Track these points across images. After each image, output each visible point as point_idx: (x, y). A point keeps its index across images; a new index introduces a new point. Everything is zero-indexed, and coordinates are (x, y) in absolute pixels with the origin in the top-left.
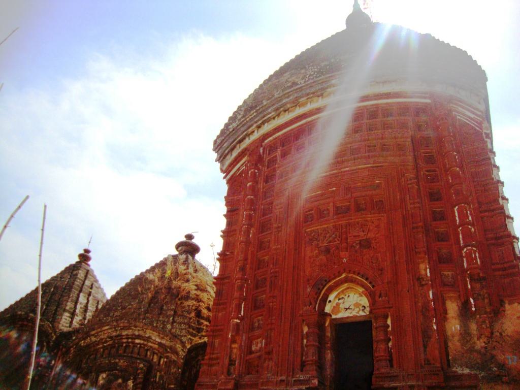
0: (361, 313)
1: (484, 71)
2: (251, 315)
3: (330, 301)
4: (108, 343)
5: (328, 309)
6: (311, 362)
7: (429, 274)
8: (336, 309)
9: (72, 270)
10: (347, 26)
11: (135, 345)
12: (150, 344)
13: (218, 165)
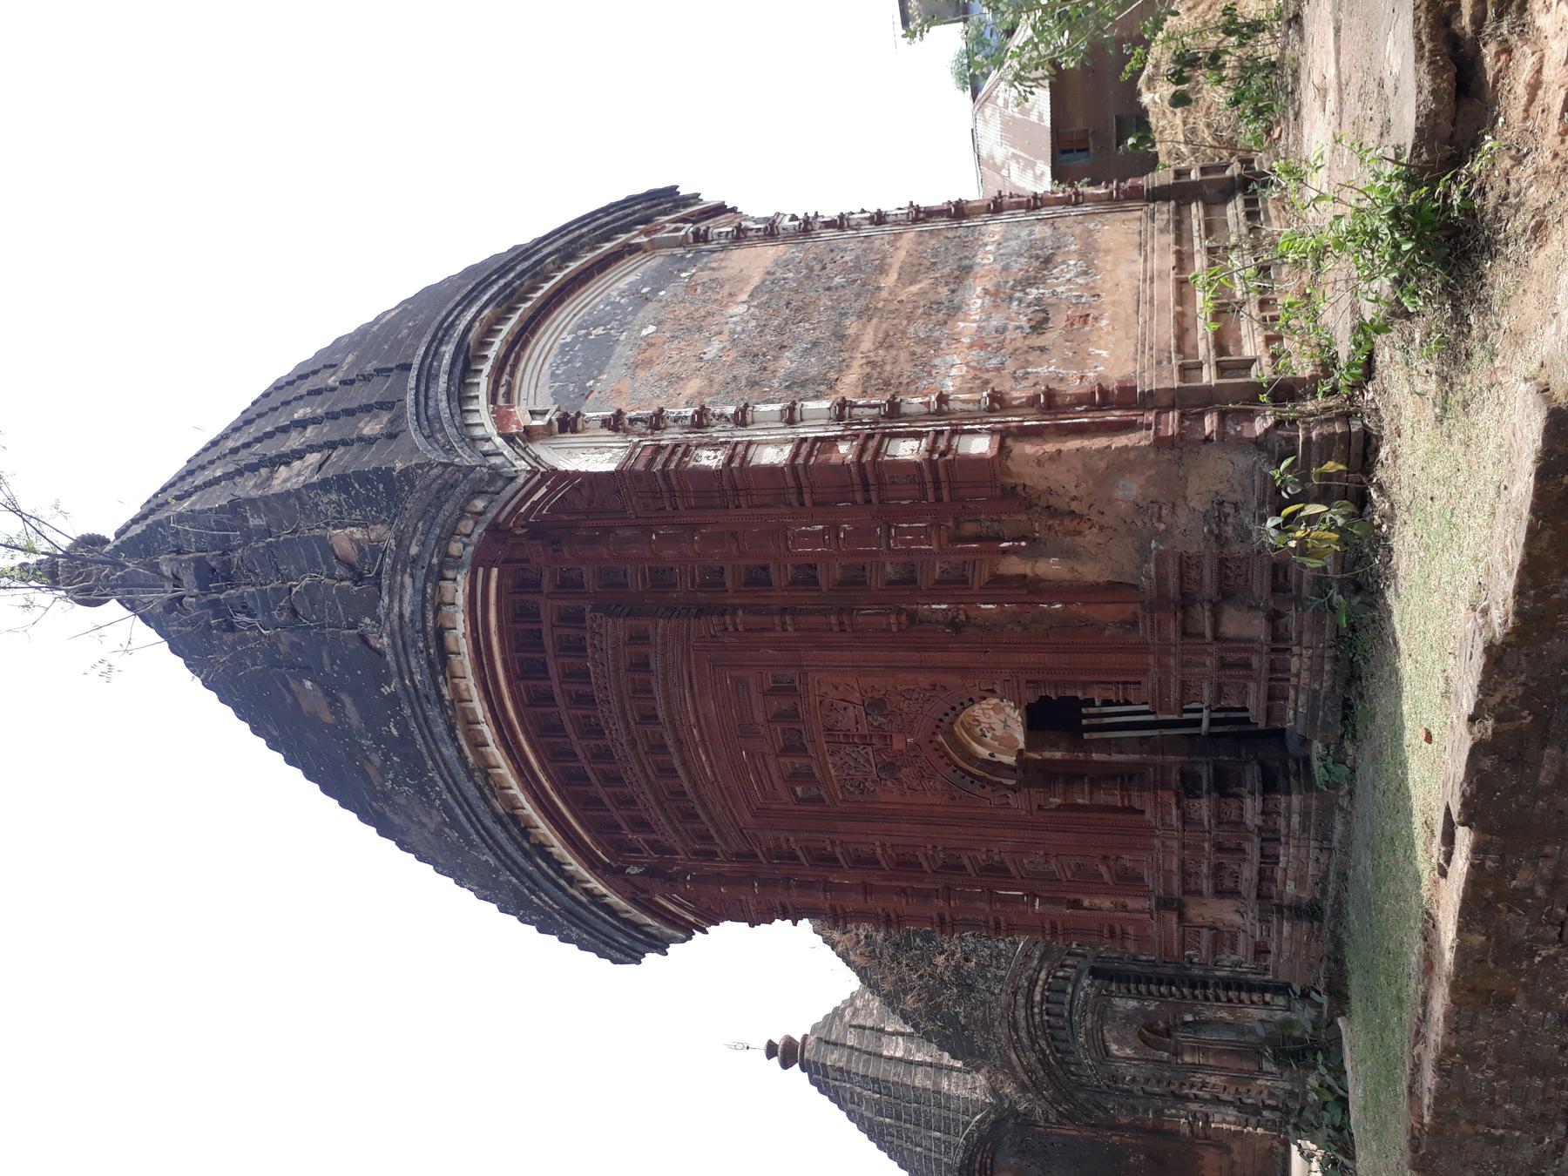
2: (1023, 878)
3: (992, 755)
4: (1044, 1046)
5: (1009, 760)
6: (1126, 800)
7: (944, 607)
8: (1007, 742)
9: (825, 1080)
12: (1043, 975)
13: (673, 948)
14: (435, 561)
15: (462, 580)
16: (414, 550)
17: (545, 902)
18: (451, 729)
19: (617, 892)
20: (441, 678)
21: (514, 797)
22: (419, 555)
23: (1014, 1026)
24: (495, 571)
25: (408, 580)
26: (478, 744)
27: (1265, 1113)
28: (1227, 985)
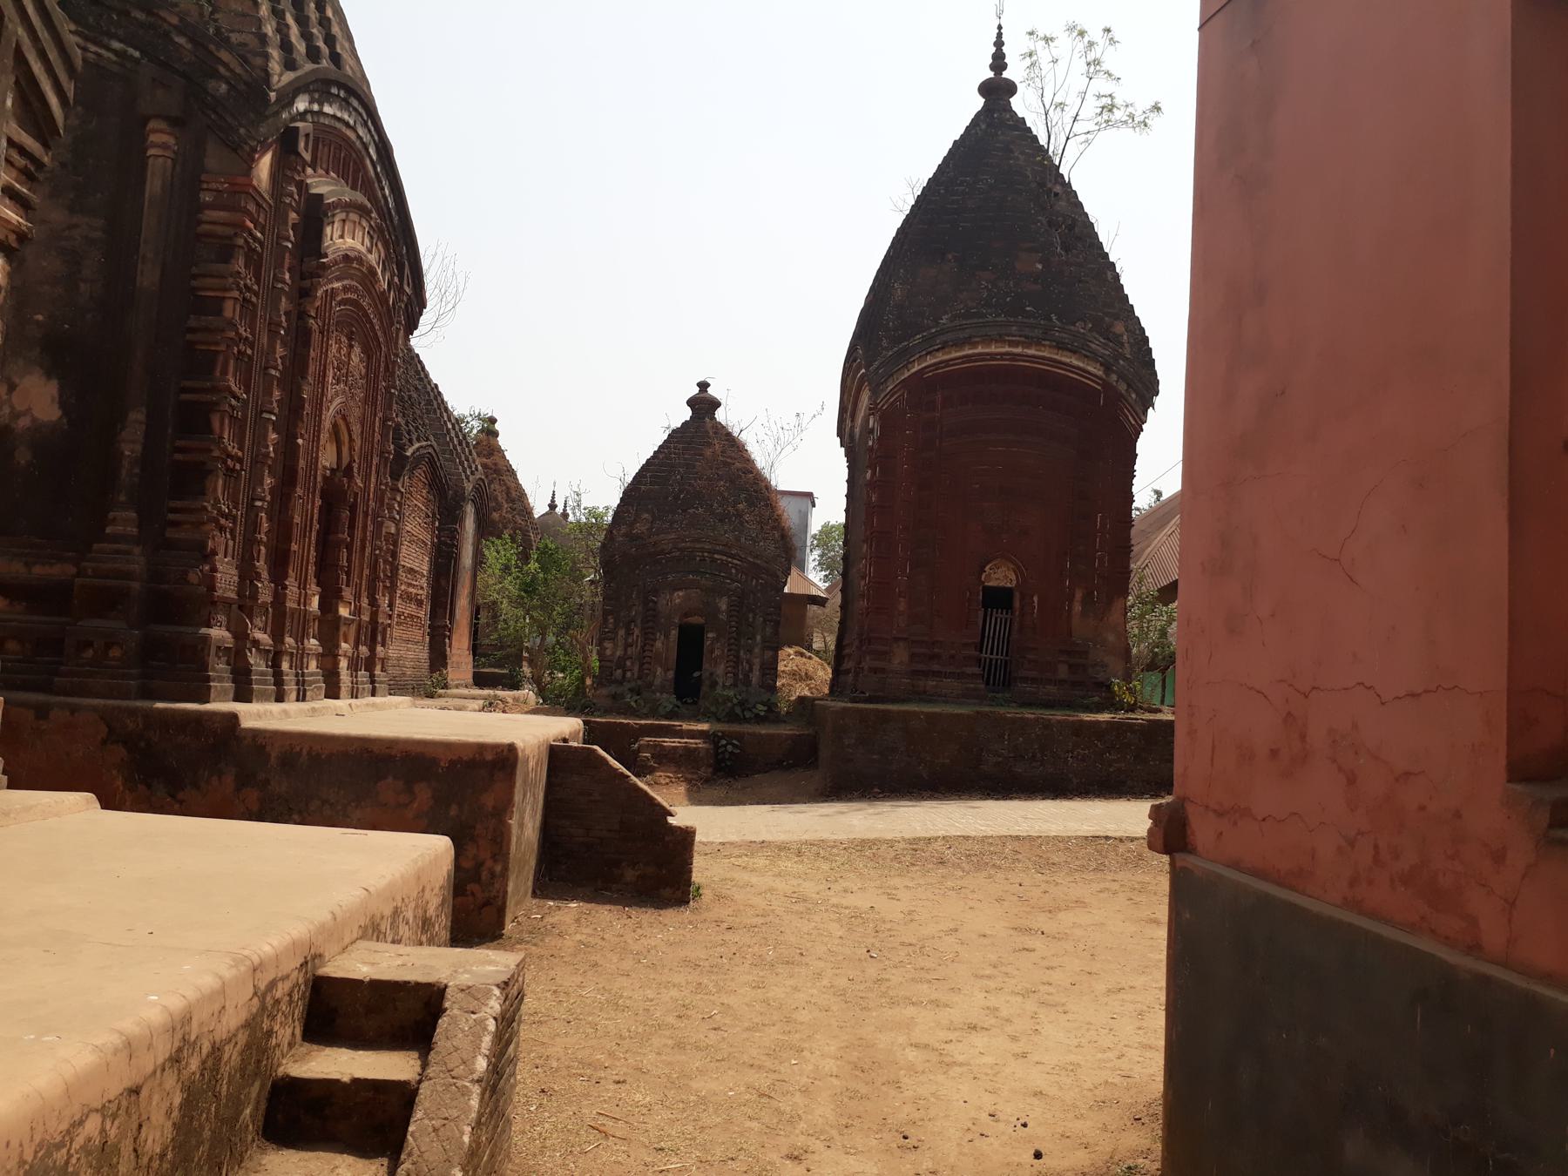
0: (1009, 585)
1: (1147, 338)
10: (984, 97)
11: (714, 560)
14: (1114, 368)
15: (1100, 373)
16: (1121, 362)
17: (915, 340)
18: (1026, 337)
19: (909, 376)
20: (1054, 344)
21: (976, 348)
22: (1119, 363)
23: (698, 540)
24: (1099, 388)
25: (1107, 353)
26: (1011, 344)
27: (619, 671)
28: (738, 657)
